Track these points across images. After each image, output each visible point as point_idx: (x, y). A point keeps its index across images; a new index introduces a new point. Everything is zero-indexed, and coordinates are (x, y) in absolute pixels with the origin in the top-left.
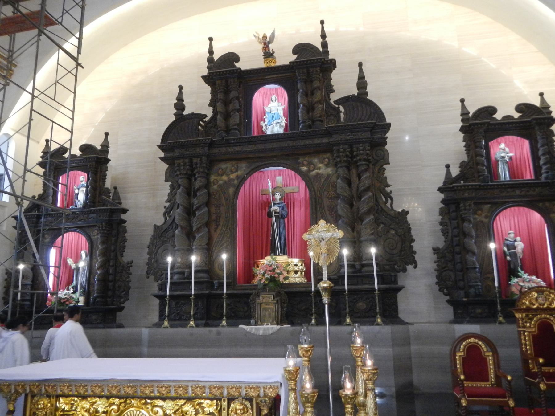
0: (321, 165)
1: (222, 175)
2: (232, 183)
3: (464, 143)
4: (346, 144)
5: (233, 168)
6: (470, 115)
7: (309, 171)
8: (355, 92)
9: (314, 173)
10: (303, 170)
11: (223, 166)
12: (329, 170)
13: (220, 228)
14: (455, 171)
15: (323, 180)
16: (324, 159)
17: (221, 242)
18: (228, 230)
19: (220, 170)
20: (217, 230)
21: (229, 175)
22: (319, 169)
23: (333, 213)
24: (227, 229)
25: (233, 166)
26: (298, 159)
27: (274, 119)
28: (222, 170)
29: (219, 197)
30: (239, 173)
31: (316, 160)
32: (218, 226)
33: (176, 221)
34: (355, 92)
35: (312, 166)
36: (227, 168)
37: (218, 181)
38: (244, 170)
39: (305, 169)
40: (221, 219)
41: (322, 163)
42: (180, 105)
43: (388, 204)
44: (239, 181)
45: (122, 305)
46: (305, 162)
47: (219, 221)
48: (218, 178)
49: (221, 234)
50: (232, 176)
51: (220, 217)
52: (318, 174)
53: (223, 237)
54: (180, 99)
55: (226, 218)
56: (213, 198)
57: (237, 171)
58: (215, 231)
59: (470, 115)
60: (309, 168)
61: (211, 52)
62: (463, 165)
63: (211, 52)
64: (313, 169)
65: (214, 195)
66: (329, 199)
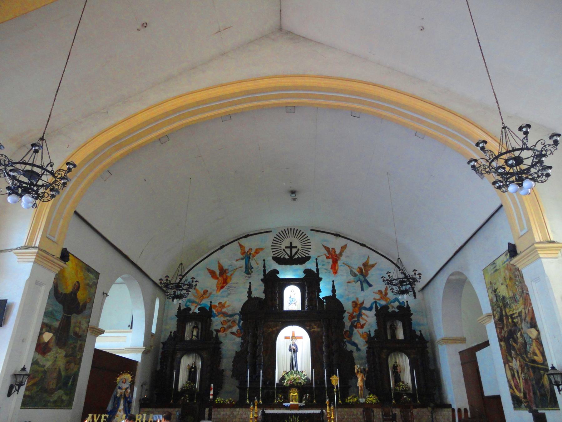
0: (315, 327)
3: (376, 321)
6: (379, 309)
8: (331, 294)
12: (319, 330)
14: (373, 334)
22: (314, 328)
27: (293, 301)
31: (313, 324)
33: (249, 349)
34: (331, 294)
41: (315, 325)
42: (250, 292)
43: (345, 347)
45: (219, 392)
50: (274, 329)
52: (314, 331)
54: (250, 288)
59: (379, 309)
61: (264, 266)
62: (376, 331)
63: (264, 266)
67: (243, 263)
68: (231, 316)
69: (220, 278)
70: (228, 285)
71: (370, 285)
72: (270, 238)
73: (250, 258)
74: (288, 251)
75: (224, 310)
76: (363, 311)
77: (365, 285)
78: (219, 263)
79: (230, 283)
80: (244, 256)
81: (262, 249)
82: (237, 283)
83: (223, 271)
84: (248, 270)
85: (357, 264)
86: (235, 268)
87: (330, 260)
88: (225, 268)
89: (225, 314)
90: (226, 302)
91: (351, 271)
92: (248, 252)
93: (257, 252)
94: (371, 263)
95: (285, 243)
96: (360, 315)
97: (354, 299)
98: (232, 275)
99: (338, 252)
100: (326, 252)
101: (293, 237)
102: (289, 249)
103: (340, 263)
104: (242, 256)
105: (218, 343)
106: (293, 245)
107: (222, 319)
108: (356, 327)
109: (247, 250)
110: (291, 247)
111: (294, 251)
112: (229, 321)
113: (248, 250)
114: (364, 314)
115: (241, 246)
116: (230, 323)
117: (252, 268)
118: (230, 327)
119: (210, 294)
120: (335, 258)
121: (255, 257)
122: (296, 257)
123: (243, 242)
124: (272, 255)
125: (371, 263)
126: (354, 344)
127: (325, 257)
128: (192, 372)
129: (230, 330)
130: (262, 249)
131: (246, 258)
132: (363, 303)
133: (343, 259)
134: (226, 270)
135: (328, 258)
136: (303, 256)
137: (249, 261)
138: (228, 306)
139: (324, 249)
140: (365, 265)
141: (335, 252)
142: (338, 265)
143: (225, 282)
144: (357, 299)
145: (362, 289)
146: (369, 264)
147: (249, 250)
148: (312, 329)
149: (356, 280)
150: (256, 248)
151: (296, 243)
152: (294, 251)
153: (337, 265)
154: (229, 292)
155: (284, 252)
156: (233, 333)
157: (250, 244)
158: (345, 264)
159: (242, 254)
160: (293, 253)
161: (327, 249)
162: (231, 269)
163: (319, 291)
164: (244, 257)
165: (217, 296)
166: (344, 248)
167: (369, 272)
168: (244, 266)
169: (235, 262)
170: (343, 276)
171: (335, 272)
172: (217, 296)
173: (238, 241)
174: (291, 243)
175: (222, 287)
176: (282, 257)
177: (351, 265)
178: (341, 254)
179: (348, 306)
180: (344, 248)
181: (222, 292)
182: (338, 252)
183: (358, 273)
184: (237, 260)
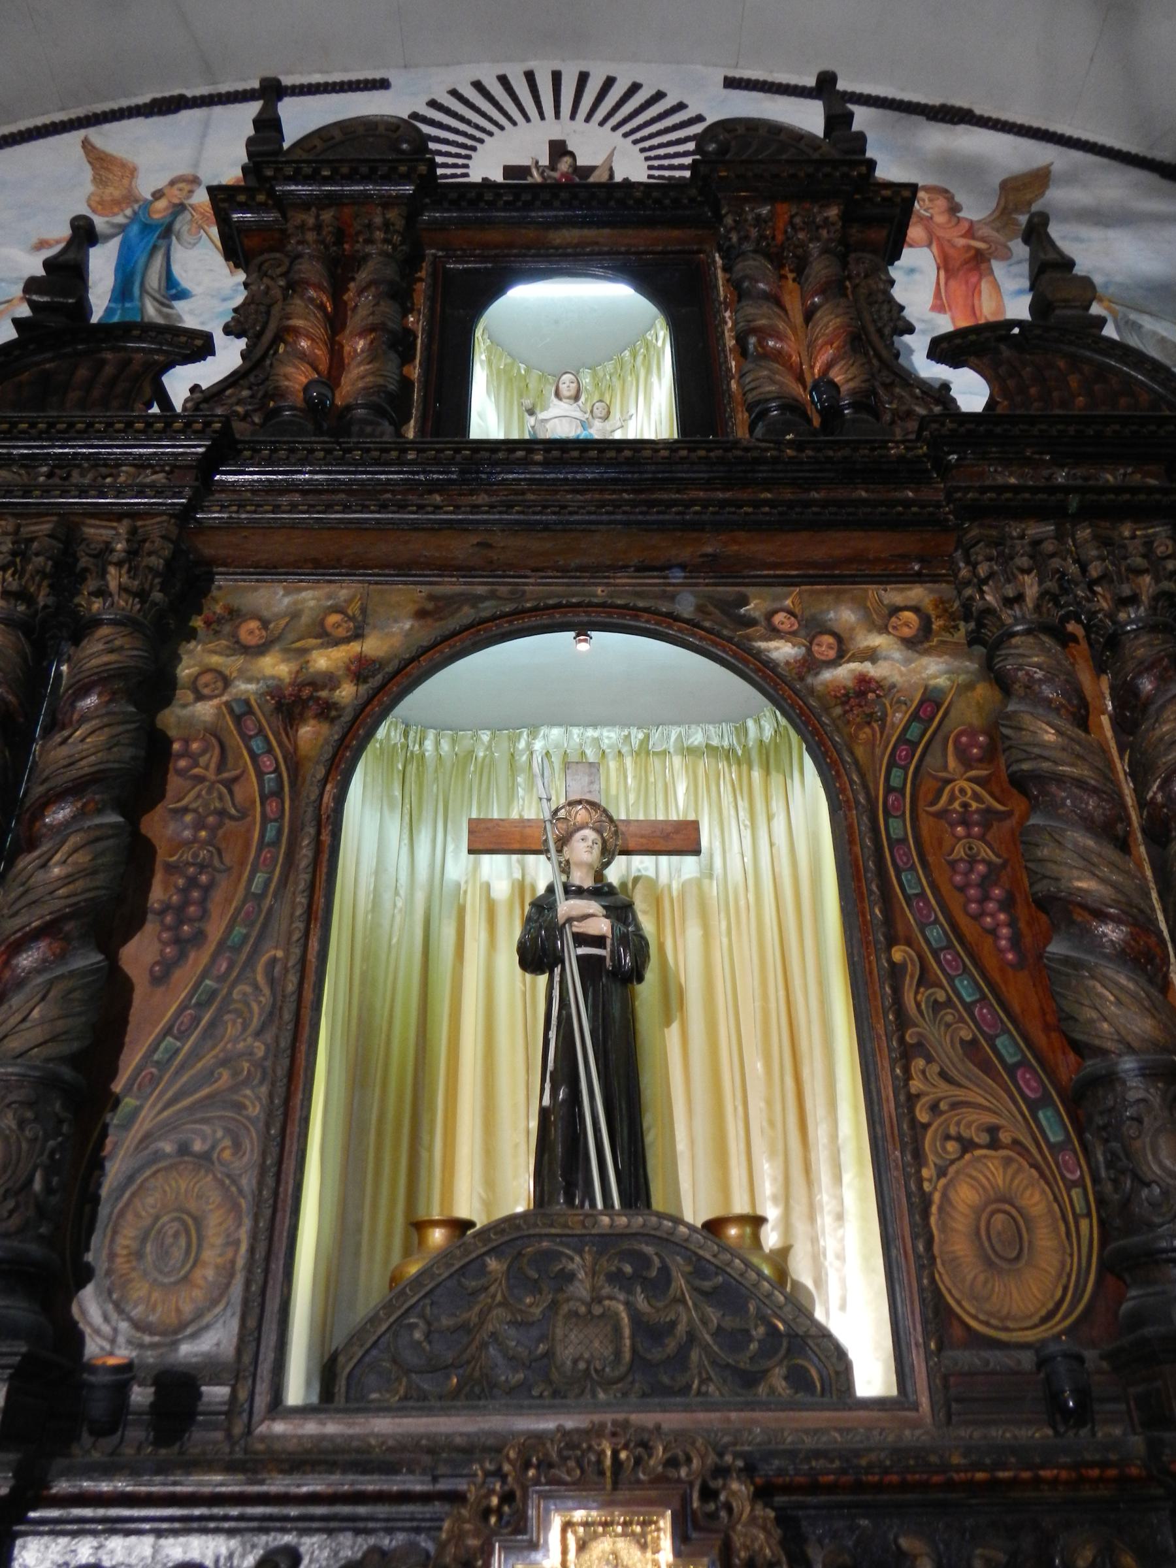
0: (877, 640)
1: (261, 650)
2: (324, 694)
4: (1040, 513)
5: (334, 618)
7: (810, 664)
9: (844, 673)
10: (775, 655)
13: (198, 959)
15: (899, 718)
16: (895, 610)
17: (195, 1055)
18: (260, 978)
19: (254, 624)
20: (177, 974)
21: (304, 651)
22: (871, 656)
23: (991, 906)
24: (251, 961)
25: (336, 609)
26: (744, 601)
28: (265, 624)
29: (222, 766)
30: (373, 646)
31: (845, 616)
32: (184, 945)
35: (828, 639)
36: (295, 615)
37: (227, 682)
38: (408, 634)
39: (783, 651)
40: (214, 908)
41: (883, 629)
44: (363, 688)
46: (779, 618)
47: (205, 915)
48: (230, 664)
49: (202, 1006)
51: (207, 889)
52: (863, 680)
53: (212, 1024)
55: (248, 895)
56: (181, 773)
57: (358, 635)
58: (162, 976)
60: (809, 650)
64: (832, 654)
65: (186, 754)
66: (953, 825)
73: (167, 231)
80: (120, 219)
92: (158, 195)
101: (573, 116)
113: (161, 182)
120: (962, 242)
131: (135, 229)
137: (155, 248)
141: (954, 208)
142: (996, 286)
147: (172, 183)
148: (842, 656)
153: (985, 286)
164: (114, 225)
173: (81, 134)
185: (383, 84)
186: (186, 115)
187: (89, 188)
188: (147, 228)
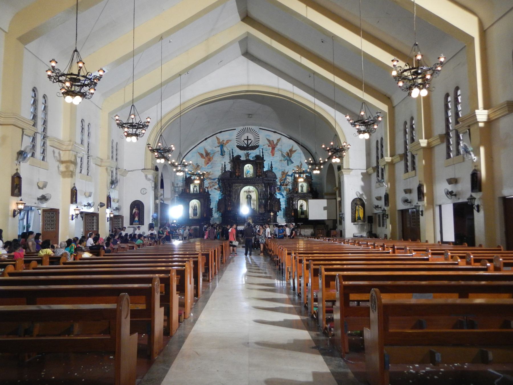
11: (236, 184)
67: (219, 149)
68: (214, 179)
69: (206, 158)
70: (211, 162)
71: (292, 163)
72: (235, 133)
74: (246, 141)
75: (210, 176)
76: (287, 177)
77: (289, 162)
78: (205, 149)
79: (213, 160)
81: (230, 141)
82: (216, 161)
83: (207, 154)
84: (222, 153)
85: (286, 150)
86: (215, 152)
87: (271, 148)
88: (208, 152)
89: (210, 179)
90: (210, 172)
91: (282, 154)
93: (228, 141)
94: (293, 150)
95: (244, 137)
96: (285, 179)
97: (283, 170)
98: (213, 156)
99: (275, 143)
100: (268, 143)
102: (247, 141)
103: (276, 149)
104: (218, 145)
105: (208, 194)
106: (249, 138)
107: (209, 181)
108: (283, 185)
109: (221, 141)
110: (248, 140)
111: (249, 141)
112: (213, 182)
114: (288, 179)
115: (217, 138)
116: (213, 184)
117: (225, 152)
118: (214, 185)
119: (201, 167)
121: (226, 146)
122: (251, 145)
123: (218, 135)
124: (236, 144)
125: (293, 150)
126: (282, 195)
127: (267, 146)
128: (195, 209)
129: (214, 187)
130: (230, 141)
132: (288, 172)
133: (278, 147)
134: (209, 153)
135: (269, 146)
136: (255, 145)
138: (212, 174)
139: (267, 140)
140: (291, 151)
141: (273, 143)
143: (209, 160)
144: (285, 170)
145: (288, 165)
146: (293, 150)
149: (284, 160)
150: (227, 139)
151: (251, 137)
152: (249, 141)
154: (212, 166)
155: (243, 143)
156: (215, 189)
157: (223, 137)
158: (279, 150)
159: (218, 143)
160: (249, 144)
161: (269, 141)
162: (212, 153)
163: (264, 167)
165: (205, 168)
166: (279, 140)
167: (292, 155)
168: (220, 151)
169: (214, 148)
170: (278, 156)
171: (273, 155)
172: (205, 168)
174: (248, 137)
175: (208, 163)
176: (242, 146)
177: (282, 151)
178: (277, 144)
179: (279, 175)
180: (279, 140)
181: (208, 166)
182: (275, 143)
183: (286, 156)
184: (215, 147)
185: (235, 129)
186: (222, 133)
187: (217, 141)
188: (222, 145)
